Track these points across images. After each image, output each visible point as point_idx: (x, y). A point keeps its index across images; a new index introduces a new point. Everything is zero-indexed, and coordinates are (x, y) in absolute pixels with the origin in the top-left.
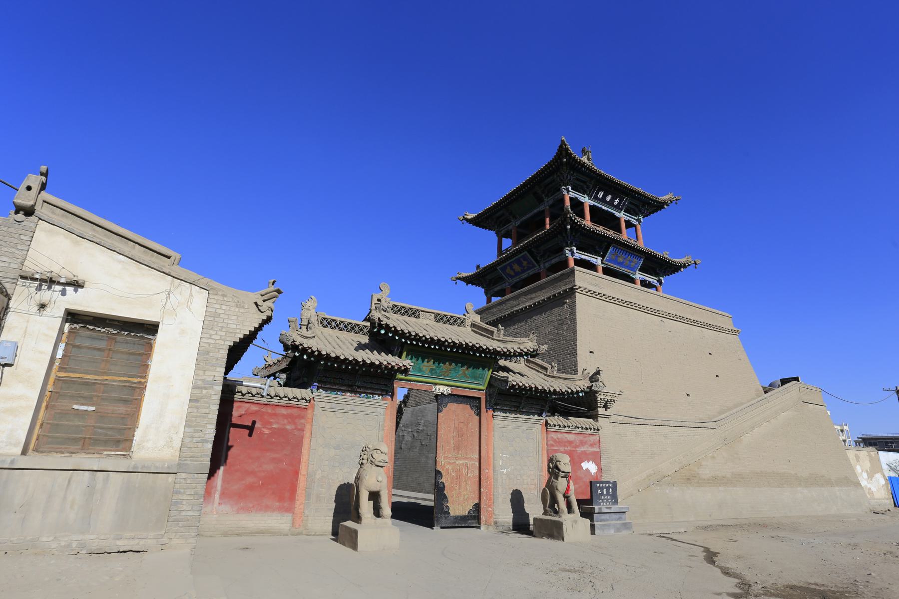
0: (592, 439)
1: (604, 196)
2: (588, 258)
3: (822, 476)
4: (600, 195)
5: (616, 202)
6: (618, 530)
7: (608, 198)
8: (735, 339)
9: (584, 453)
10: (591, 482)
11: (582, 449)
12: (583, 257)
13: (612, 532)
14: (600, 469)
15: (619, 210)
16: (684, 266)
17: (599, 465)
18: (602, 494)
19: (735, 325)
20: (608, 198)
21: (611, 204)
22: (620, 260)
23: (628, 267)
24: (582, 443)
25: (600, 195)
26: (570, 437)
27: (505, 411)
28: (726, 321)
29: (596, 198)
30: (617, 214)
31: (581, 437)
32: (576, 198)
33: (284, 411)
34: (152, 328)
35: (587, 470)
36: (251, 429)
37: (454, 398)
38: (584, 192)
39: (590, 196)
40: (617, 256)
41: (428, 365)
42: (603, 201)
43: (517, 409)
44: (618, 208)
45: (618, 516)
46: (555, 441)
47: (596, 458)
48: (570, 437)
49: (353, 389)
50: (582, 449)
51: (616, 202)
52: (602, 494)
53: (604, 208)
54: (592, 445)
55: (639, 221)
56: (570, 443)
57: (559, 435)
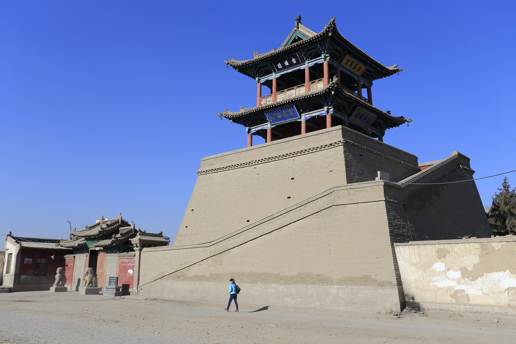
0: (133, 260)
1: (283, 64)
2: (260, 128)
4: (280, 66)
5: (294, 61)
6: (110, 295)
7: (287, 63)
9: (129, 266)
10: (110, 277)
11: (129, 264)
12: (258, 129)
13: (108, 295)
14: (133, 273)
15: (303, 62)
17: (133, 271)
20: (287, 63)
21: (291, 65)
22: (280, 116)
23: (290, 117)
24: (129, 262)
25: (280, 66)
26: (126, 260)
29: (279, 70)
30: (302, 67)
31: (129, 260)
37: (100, 251)
38: (269, 72)
42: (285, 67)
43: (112, 252)
44: (298, 63)
47: (132, 268)
48: (126, 260)
50: (129, 264)
53: (290, 71)
56: (125, 262)
57: (123, 260)
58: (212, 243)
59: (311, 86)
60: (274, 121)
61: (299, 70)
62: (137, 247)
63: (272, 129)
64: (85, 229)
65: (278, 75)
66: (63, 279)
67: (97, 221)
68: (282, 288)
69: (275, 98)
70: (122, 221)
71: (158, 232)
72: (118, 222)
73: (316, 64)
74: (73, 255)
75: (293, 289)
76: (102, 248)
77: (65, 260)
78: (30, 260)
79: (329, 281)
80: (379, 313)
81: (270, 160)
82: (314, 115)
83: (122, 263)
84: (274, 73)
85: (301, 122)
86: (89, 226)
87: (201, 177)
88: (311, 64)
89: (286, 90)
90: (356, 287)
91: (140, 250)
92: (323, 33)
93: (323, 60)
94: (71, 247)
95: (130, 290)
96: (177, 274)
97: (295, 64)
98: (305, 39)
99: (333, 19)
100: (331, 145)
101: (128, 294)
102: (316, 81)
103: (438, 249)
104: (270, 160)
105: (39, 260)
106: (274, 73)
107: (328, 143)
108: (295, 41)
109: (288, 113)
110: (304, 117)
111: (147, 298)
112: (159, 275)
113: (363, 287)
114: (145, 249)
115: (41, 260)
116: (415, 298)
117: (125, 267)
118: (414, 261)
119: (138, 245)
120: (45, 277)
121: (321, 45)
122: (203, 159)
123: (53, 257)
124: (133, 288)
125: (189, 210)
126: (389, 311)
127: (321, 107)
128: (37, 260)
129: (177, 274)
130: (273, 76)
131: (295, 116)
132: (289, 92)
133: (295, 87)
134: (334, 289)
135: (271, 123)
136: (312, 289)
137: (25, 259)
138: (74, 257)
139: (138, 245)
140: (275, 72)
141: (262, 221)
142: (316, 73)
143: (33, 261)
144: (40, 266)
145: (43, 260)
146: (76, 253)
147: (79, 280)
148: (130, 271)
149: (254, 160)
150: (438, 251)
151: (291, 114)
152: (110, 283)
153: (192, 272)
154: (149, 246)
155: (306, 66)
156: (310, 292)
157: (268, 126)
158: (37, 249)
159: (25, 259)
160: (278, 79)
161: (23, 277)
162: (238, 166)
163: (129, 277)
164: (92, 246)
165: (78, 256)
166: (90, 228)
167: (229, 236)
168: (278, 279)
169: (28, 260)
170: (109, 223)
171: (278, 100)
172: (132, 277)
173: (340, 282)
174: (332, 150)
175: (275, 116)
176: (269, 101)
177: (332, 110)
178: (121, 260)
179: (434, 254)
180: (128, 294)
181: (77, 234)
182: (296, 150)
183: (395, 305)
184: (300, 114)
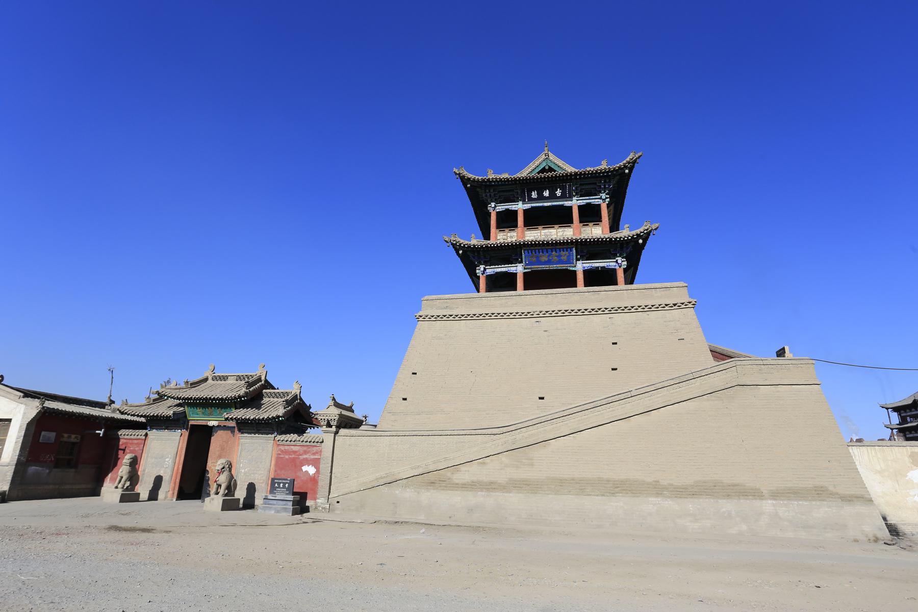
0: (315, 449)
3: (734, 485)
4: (534, 195)
5: (559, 193)
6: (278, 512)
7: (546, 194)
8: (691, 312)
9: (306, 459)
10: (273, 480)
11: (305, 456)
13: (273, 512)
14: (318, 471)
15: (570, 198)
16: (646, 236)
18: (279, 487)
19: (690, 296)
21: (553, 197)
22: (544, 259)
24: (305, 452)
25: (534, 195)
27: (250, 433)
28: (678, 292)
29: (531, 200)
30: (567, 203)
31: (305, 448)
32: (507, 210)
33: (136, 442)
34: (10, 420)
35: (306, 472)
36: (124, 450)
39: (524, 202)
40: (538, 257)
41: (199, 410)
42: (541, 198)
43: (258, 431)
44: (563, 197)
45: (284, 503)
46: (282, 451)
47: (316, 463)
49: (167, 428)
50: (305, 456)
51: (559, 193)
52: (279, 487)
53: (546, 204)
54: (314, 454)
55: (601, 198)
56: (295, 452)
57: (286, 448)
58: (507, 429)
59: (583, 229)
60: (531, 263)
61: (562, 205)
62: (329, 425)
63: (525, 275)
64: (184, 386)
65: (528, 206)
66: (134, 478)
67: (204, 376)
68: (670, 504)
69: (524, 236)
70: (266, 381)
71: (349, 405)
72: (259, 380)
73: (589, 204)
74: (144, 432)
75: (691, 505)
76: (233, 424)
77: (119, 439)
78: (52, 435)
79: (756, 494)
80: (856, 541)
81: (566, 313)
82: (597, 265)
83: (286, 452)
84: (520, 203)
85: (575, 272)
86: (191, 380)
87: (422, 325)
88: (583, 201)
89: (540, 227)
90: (805, 503)
91: (336, 433)
92: (619, 168)
93: (602, 200)
94: (144, 416)
95: (308, 503)
96: (432, 479)
97: (559, 198)
98: (560, 172)
99: (640, 154)
100: (675, 305)
101: (306, 510)
102: (591, 224)
103: (912, 452)
104: (566, 313)
105: (66, 435)
106: (520, 203)
107: (671, 302)
108: (543, 171)
109: (559, 256)
110: (580, 266)
111: (377, 519)
112: (382, 478)
113: (818, 503)
114: (342, 431)
115: (69, 437)
116: (888, 519)
117: (294, 460)
118: (878, 468)
119: (334, 423)
120: (73, 470)
121: (605, 182)
122: (426, 297)
123: (101, 432)
124: (315, 499)
125: (404, 373)
126: (872, 538)
127: (614, 256)
128: (63, 437)
129: (432, 479)
130: (520, 207)
131: (569, 261)
132: (546, 231)
133: (557, 226)
134: (768, 505)
135: (527, 265)
136: (727, 506)
137: (43, 433)
138: (146, 435)
139: (334, 423)
140: (524, 201)
141: (610, 400)
142: (590, 215)
143: (57, 437)
144: (72, 450)
145: (73, 436)
146: (152, 428)
147: (158, 481)
148: (310, 470)
149: (539, 309)
150: (912, 456)
151: (564, 258)
152: (273, 489)
153: (465, 475)
154: (345, 427)
155: (575, 203)
156: (724, 510)
157: (519, 269)
158: (72, 414)
159: (43, 433)
160: (526, 212)
161: (32, 469)
162: (503, 316)
163: (304, 478)
164: (197, 418)
165: (153, 434)
166: (192, 384)
167: (543, 419)
168: (658, 489)
169: (48, 436)
170: (251, 380)
171: (527, 239)
172: (314, 480)
173: (776, 495)
174: (676, 313)
175: (538, 257)
176: (511, 237)
177: (625, 263)
178: (282, 448)
179: (906, 459)
180: (306, 510)
181: (168, 392)
182: (616, 305)
183: (880, 529)
184: (578, 260)
